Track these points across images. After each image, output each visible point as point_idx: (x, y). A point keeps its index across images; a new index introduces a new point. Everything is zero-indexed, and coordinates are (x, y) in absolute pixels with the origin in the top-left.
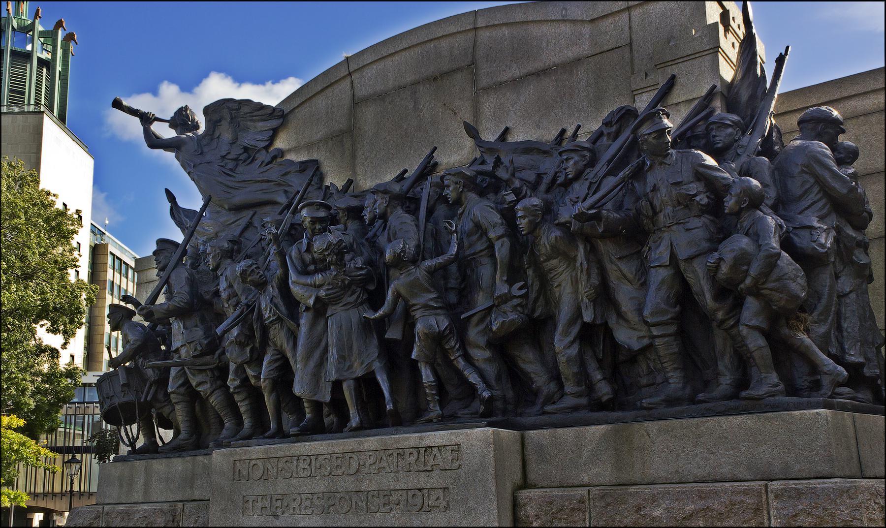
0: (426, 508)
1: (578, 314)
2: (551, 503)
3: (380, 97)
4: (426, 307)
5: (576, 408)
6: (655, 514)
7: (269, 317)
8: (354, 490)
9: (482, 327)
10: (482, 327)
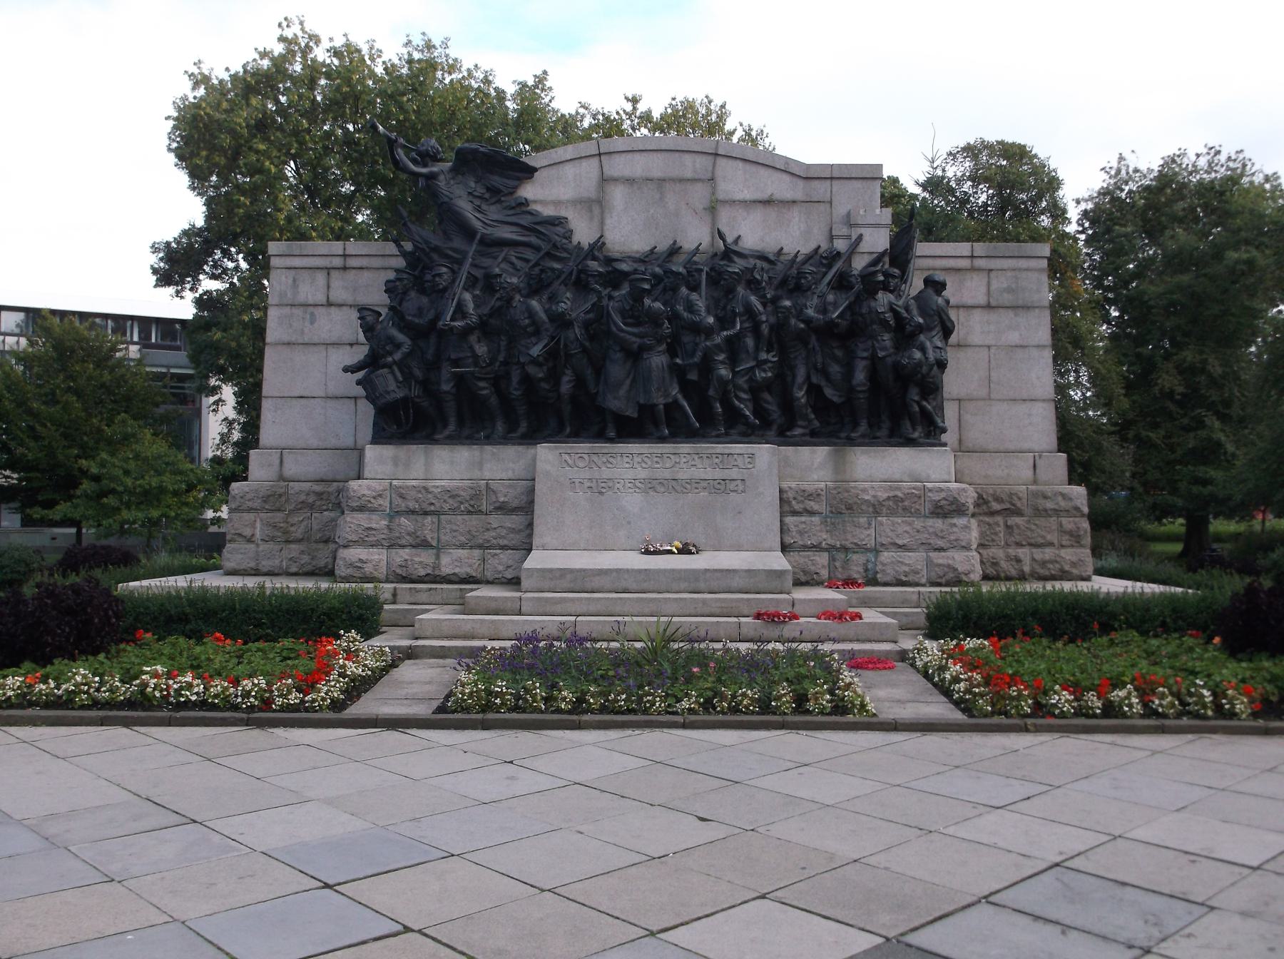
1: (808, 377)
3: (630, 181)
4: (722, 362)
5: (803, 435)
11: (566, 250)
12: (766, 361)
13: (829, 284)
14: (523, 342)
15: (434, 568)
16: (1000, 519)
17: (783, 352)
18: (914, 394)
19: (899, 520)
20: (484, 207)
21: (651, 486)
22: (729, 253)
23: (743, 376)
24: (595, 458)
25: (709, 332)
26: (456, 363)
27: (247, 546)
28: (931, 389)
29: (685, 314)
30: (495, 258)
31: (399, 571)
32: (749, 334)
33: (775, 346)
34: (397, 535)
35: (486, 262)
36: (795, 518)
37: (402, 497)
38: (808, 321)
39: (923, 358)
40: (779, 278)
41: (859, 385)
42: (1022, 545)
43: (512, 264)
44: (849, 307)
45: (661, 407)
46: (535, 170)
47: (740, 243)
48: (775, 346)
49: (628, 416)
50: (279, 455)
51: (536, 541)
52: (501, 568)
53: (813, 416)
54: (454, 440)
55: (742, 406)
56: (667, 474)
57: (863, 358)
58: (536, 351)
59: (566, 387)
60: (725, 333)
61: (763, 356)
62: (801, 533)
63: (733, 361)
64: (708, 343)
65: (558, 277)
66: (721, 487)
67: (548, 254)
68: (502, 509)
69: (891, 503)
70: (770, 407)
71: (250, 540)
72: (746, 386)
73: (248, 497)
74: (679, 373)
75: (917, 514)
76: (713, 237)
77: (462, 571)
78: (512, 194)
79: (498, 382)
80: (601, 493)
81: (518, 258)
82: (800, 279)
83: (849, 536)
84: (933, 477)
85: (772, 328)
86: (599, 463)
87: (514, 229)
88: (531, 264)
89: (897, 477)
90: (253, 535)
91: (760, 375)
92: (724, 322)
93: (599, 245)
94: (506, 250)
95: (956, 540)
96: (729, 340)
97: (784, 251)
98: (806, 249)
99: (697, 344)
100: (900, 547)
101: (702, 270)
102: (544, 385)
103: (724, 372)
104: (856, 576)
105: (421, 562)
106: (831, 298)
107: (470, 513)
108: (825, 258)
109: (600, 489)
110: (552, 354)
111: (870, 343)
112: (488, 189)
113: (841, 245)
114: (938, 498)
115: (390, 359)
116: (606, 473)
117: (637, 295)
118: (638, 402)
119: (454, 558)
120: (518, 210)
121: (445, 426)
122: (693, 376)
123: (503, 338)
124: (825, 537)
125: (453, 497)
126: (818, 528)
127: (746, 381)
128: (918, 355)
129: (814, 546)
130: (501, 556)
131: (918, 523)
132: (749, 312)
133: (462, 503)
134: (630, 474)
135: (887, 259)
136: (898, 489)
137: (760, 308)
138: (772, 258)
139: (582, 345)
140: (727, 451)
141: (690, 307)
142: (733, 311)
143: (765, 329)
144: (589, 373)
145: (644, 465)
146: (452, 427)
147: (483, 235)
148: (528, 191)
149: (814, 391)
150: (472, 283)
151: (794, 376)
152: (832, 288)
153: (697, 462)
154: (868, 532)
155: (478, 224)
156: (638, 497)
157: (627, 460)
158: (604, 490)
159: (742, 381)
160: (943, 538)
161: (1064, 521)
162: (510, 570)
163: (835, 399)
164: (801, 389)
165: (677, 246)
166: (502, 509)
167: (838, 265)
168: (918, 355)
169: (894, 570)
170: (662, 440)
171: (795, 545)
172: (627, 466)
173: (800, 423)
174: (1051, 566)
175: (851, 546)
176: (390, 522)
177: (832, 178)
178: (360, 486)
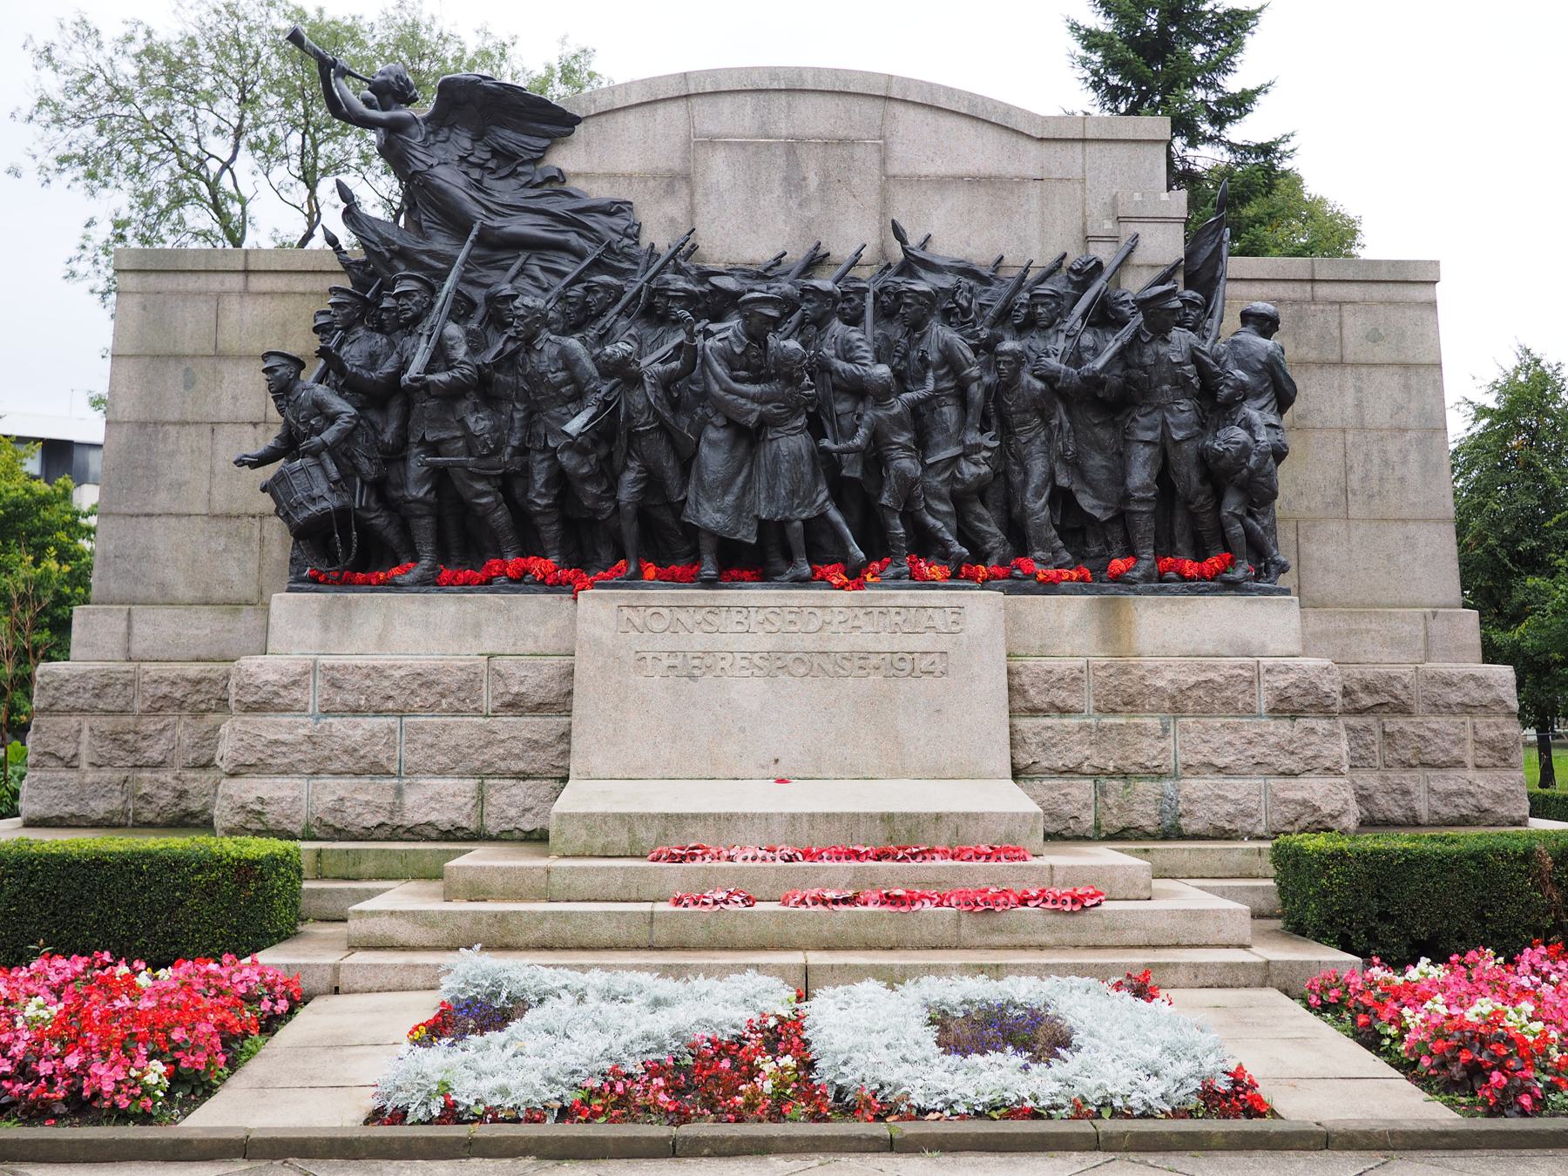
0: (917, 673)
1: (1051, 476)
4: (904, 447)
6: (1158, 685)
11: (628, 257)
12: (978, 448)
13: (1084, 316)
14: (554, 412)
15: (392, 812)
16: (1370, 720)
17: (1006, 431)
18: (1232, 504)
19: (1218, 722)
20: (488, 182)
21: (776, 664)
22: (912, 264)
24: (682, 615)
25: (881, 394)
27: (62, 775)
28: (1260, 495)
29: (840, 365)
30: (506, 269)
31: (329, 819)
33: (994, 422)
34: (326, 753)
35: (493, 276)
36: (1034, 720)
37: (335, 685)
38: (1049, 378)
39: (1251, 441)
40: (997, 305)
41: (1137, 489)
42: (1411, 766)
43: (535, 279)
44: (1122, 354)
45: (798, 524)
46: (577, 120)
47: (930, 248)
48: (994, 422)
49: (739, 542)
50: (125, 613)
51: (575, 765)
52: (512, 812)
53: (1060, 543)
54: (431, 582)
55: (939, 524)
56: (809, 643)
57: (1147, 443)
58: (575, 425)
59: (627, 491)
60: (909, 395)
61: (973, 437)
62: (1044, 746)
63: (922, 445)
64: (880, 413)
65: (617, 300)
66: (901, 665)
67: (598, 265)
68: (514, 705)
69: (1201, 693)
70: (985, 527)
71: (70, 764)
72: (945, 491)
73: (70, 687)
74: (827, 464)
75: (1250, 711)
77: (443, 817)
78: (535, 161)
79: (509, 485)
80: (692, 677)
81: (543, 269)
82: (1035, 306)
83: (1129, 751)
84: (1272, 647)
85: (988, 389)
86: (689, 626)
87: (542, 220)
88: (568, 279)
89: (1209, 648)
90: (75, 756)
91: (969, 470)
93: (686, 250)
94: (524, 255)
95: (1315, 757)
96: (915, 409)
97: (1004, 262)
98: (1043, 257)
99: (860, 417)
100: (1220, 770)
101: (867, 290)
102: (592, 489)
103: (906, 463)
104: (1144, 822)
105: (367, 803)
106: (1087, 339)
108: (1077, 272)
109: (691, 669)
110: (606, 431)
111: (1157, 416)
112: (495, 153)
113: (1105, 253)
114: (1283, 684)
115: (316, 439)
116: (699, 641)
117: (756, 335)
118: (757, 517)
119: (429, 794)
120: (546, 188)
121: (416, 559)
122: (853, 471)
123: (518, 406)
124: (1088, 753)
125: (427, 685)
128: (1240, 434)
129: (1070, 771)
130: (514, 791)
131: (1250, 728)
132: (949, 359)
133: (443, 696)
134: (748, 642)
135: (1180, 277)
136: (1214, 667)
137: (970, 355)
138: (986, 273)
139: (657, 415)
141: (847, 353)
142: (923, 359)
143: (976, 391)
144: (669, 465)
145: (769, 627)
146: (425, 562)
147: (483, 228)
148: (566, 159)
149: (1062, 500)
150: (461, 309)
151: (1026, 473)
152: (1089, 324)
153: (862, 620)
155: (475, 210)
156: (759, 684)
157: (740, 617)
158: (696, 672)
160: (1292, 753)
161: (1480, 722)
162: (529, 816)
163: (1097, 513)
164: (1038, 495)
165: (822, 252)
166: (514, 705)
167: (1098, 285)
168: (1240, 434)
169: (1209, 810)
170: (801, 582)
171: (1036, 768)
172: (740, 628)
173: (1039, 554)
174: (1460, 801)
175: (1134, 769)
177: (1084, 140)
178: (260, 666)
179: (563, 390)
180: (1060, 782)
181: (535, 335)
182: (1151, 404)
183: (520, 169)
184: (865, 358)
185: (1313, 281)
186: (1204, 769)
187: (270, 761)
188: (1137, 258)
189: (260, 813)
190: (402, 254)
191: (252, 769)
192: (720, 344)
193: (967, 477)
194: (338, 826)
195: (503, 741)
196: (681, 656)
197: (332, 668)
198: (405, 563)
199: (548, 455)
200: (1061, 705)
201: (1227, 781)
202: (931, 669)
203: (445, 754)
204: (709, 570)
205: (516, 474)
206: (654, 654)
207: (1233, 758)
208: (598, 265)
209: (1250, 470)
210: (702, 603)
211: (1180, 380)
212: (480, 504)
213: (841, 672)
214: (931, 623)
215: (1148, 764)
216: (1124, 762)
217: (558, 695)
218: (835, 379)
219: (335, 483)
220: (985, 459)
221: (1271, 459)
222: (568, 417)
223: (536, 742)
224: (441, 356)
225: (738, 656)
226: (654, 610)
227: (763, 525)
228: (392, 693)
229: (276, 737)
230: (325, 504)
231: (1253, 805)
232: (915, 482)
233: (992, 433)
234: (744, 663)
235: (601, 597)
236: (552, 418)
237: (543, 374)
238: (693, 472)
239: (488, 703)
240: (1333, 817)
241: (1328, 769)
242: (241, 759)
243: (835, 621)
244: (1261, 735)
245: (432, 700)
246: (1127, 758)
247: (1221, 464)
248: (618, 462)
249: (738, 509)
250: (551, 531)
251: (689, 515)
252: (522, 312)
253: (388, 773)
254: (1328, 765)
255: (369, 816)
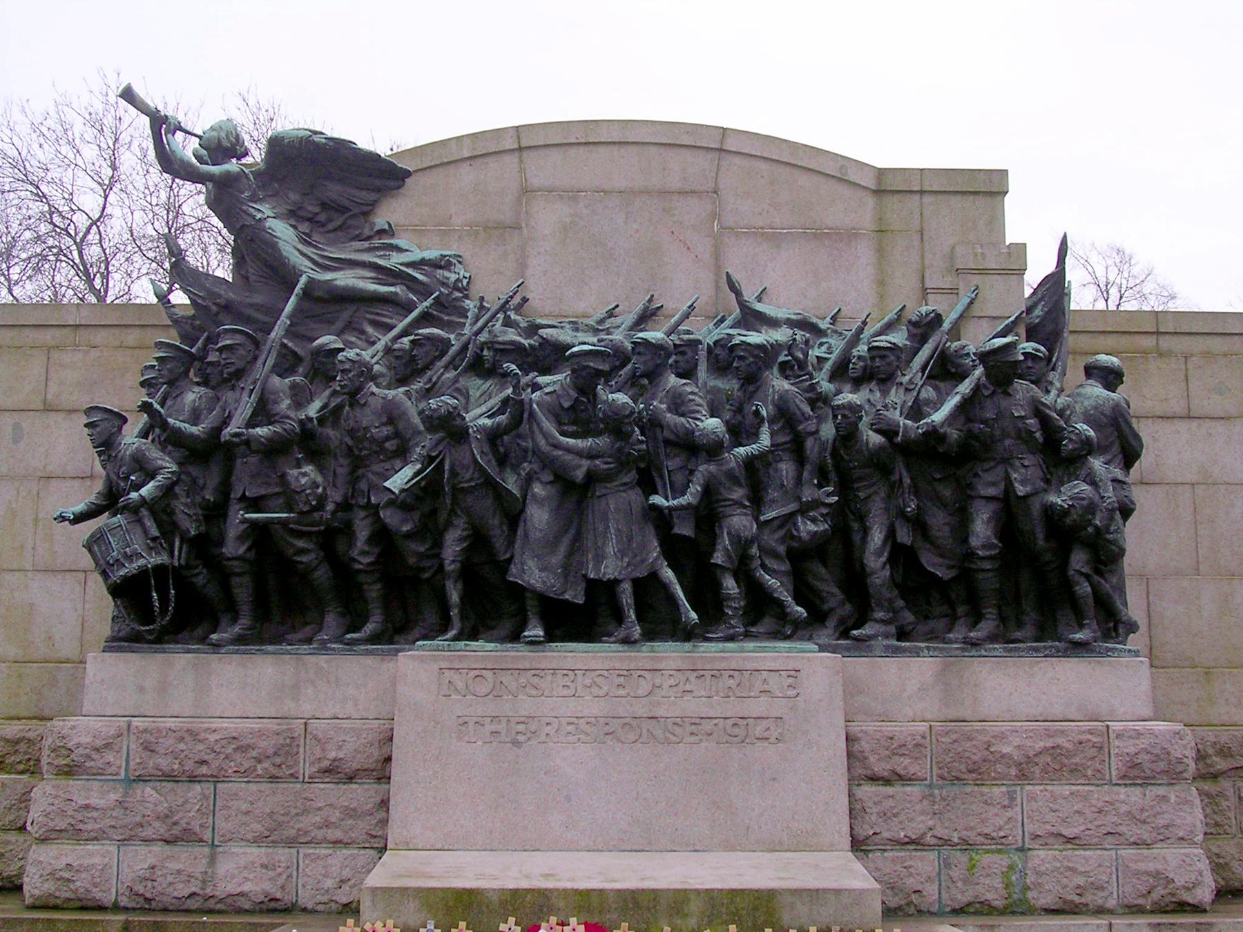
1: (891, 534)
2: (892, 738)
6: (1004, 751)
7: (471, 480)
8: (645, 715)
9: (782, 533)
10: (782, 533)
12: (816, 504)
14: (376, 468)
15: (204, 881)
17: (845, 486)
19: (1066, 790)
23: (775, 531)
24: (507, 678)
25: (713, 450)
26: (255, 504)
31: (140, 888)
32: (785, 456)
33: (833, 476)
34: (138, 819)
37: (148, 748)
38: (888, 432)
39: (1097, 497)
51: (394, 833)
52: (329, 883)
56: (640, 709)
58: (399, 480)
59: (452, 547)
63: (757, 501)
65: (443, 353)
68: (332, 772)
72: (782, 549)
75: (1099, 778)
76: (718, 288)
80: (516, 743)
89: (1057, 711)
91: (807, 528)
92: (740, 432)
95: (1167, 827)
96: (750, 464)
97: (843, 313)
100: (1069, 840)
104: (989, 896)
105: (179, 872)
106: (928, 393)
107: (274, 779)
111: (1000, 470)
112: (324, 206)
114: (1132, 750)
115: (134, 495)
116: (526, 706)
118: (585, 576)
119: (243, 863)
120: (376, 242)
121: (235, 620)
122: (684, 529)
124: (930, 823)
126: (918, 807)
127: (782, 540)
129: (912, 842)
131: (1099, 795)
133: (259, 761)
135: (1022, 331)
137: (807, 409)
140: (750, 665)
142: (757, 413)
144: (495, 524)
145: (595, 691)
146: (244, 621)
147: (311, 281)
149: (900, 556)
154: (1009, 814)
157: (567, 681)
159: (772, 539)
160: (1144, 822)
166: (332, 772)
172: (565, 692)
173: (880, 615)
175: (980, 839)
176: (126, 794)
178: (73, 728)
179: (387, 445)
180: (903, 854)
181: (358, 390)
182: (994, 459)
183: (350, 222)
184: (698, 412)
185: (1158, 333)
186: (1051, 840)
187: (81, 826)
188: (976, 310)
189: (69, 880)
190: (227, 307)
191: (63, 834)
192: (547, 398)
193: (803, 535)
194: (148, 895)
195: (319, 809)
196: (504, 721)
197: (145, 731)
198: (224, 620)
199: (372, 511)
200: (902, 773)
201: (1077, 853)
202: (766, 734)
203: (259, 822)
204: (535, 631)
205: (339, 531)
206: (476, 719)
207: (1082, 828)
208: (426, 319)
209: (1096, 528)
210: (528, 666)
211: (1024, 434)
212: (302, 563)
213: (672, 737)
214: (766, 687)
215: (994, 834)
216: (969, 834)
217: (377, 761)
218: (667, 434)
219: (154, 539)
220: (822, 515)
221: (1118, 516)
222: (393, 472)
223: (354, 810)
224: (262, 413)
225: (564, 721)
226: (477, 673)
227: (593, 586)
228: (206, 757)
229: (87, 802)
230: (141, 562)
231: (1104, 878)
232: (750, 542)
233: (831, 489)
234: (570, 728)
235: (421, 659)
236: (377, 474)
237: (366, 429)
238: (520, 532)
239: (306, 769)
240: (1188, 889)
241: (1182, 839)
242: (51, 824)
243: (665, 686)
244: (1112, 804)
245: (246, 765)
246: (972, 829)
247: (1068, 521)
248: (442, 517)
249: (566, 567)
250: (374, 591)
251: (514, 575)
252: (347, 366)
253: (201, 841)
254: (1181, 834)
255: (181, 886)
